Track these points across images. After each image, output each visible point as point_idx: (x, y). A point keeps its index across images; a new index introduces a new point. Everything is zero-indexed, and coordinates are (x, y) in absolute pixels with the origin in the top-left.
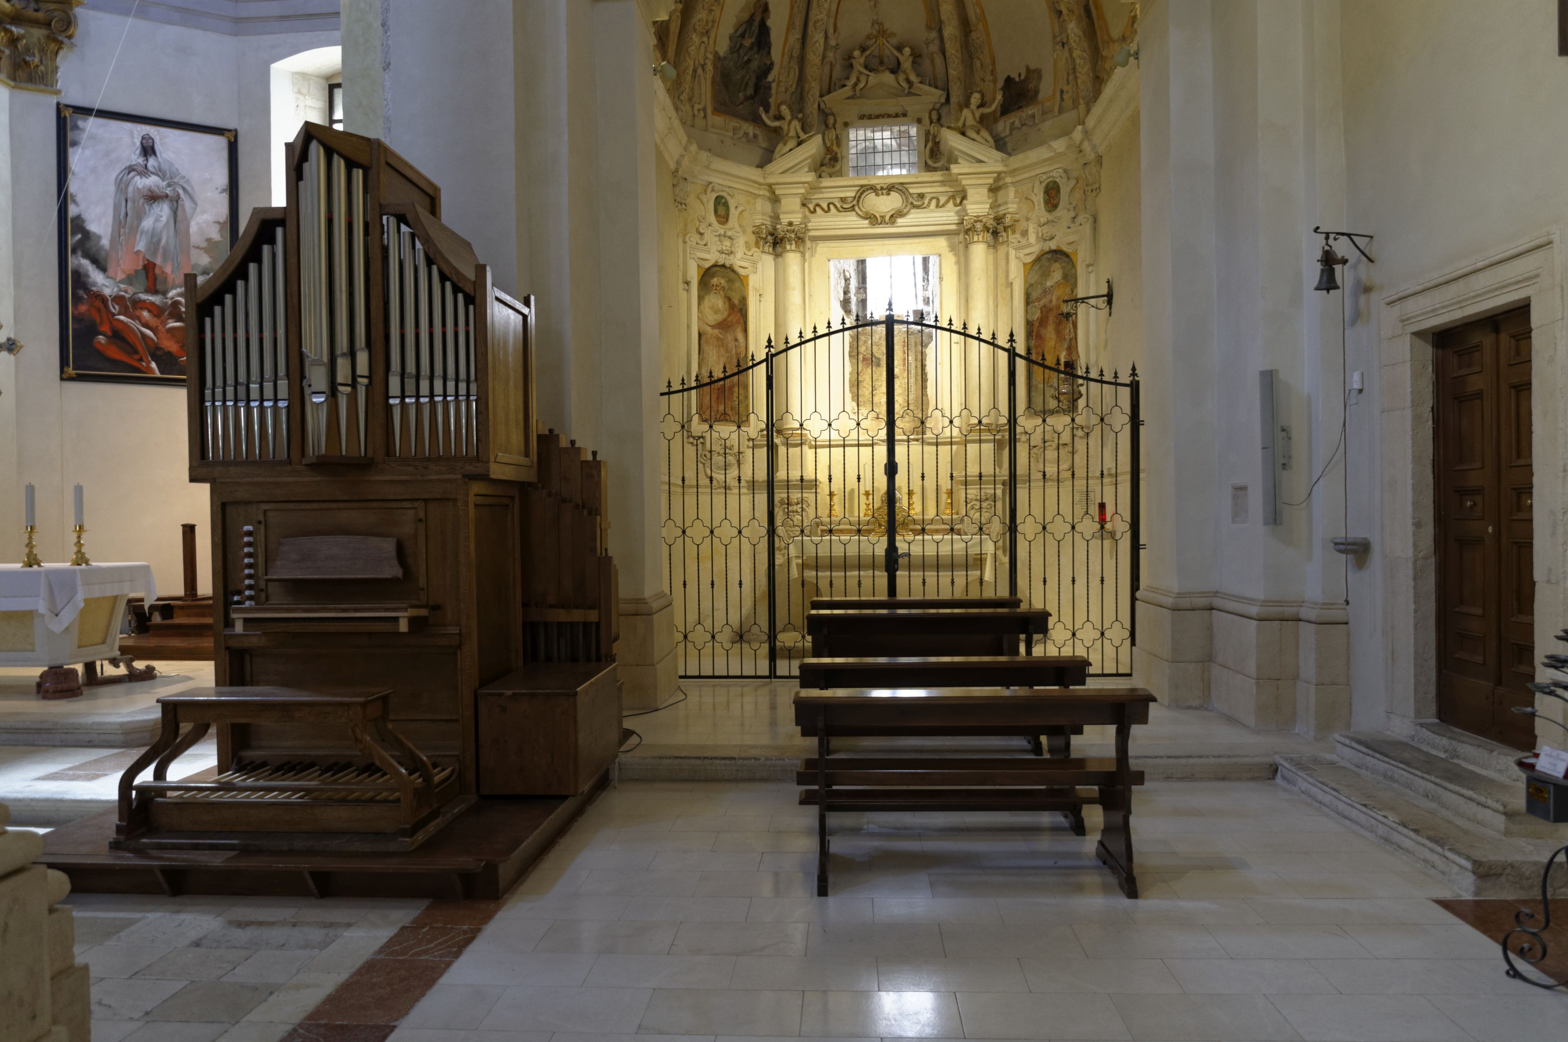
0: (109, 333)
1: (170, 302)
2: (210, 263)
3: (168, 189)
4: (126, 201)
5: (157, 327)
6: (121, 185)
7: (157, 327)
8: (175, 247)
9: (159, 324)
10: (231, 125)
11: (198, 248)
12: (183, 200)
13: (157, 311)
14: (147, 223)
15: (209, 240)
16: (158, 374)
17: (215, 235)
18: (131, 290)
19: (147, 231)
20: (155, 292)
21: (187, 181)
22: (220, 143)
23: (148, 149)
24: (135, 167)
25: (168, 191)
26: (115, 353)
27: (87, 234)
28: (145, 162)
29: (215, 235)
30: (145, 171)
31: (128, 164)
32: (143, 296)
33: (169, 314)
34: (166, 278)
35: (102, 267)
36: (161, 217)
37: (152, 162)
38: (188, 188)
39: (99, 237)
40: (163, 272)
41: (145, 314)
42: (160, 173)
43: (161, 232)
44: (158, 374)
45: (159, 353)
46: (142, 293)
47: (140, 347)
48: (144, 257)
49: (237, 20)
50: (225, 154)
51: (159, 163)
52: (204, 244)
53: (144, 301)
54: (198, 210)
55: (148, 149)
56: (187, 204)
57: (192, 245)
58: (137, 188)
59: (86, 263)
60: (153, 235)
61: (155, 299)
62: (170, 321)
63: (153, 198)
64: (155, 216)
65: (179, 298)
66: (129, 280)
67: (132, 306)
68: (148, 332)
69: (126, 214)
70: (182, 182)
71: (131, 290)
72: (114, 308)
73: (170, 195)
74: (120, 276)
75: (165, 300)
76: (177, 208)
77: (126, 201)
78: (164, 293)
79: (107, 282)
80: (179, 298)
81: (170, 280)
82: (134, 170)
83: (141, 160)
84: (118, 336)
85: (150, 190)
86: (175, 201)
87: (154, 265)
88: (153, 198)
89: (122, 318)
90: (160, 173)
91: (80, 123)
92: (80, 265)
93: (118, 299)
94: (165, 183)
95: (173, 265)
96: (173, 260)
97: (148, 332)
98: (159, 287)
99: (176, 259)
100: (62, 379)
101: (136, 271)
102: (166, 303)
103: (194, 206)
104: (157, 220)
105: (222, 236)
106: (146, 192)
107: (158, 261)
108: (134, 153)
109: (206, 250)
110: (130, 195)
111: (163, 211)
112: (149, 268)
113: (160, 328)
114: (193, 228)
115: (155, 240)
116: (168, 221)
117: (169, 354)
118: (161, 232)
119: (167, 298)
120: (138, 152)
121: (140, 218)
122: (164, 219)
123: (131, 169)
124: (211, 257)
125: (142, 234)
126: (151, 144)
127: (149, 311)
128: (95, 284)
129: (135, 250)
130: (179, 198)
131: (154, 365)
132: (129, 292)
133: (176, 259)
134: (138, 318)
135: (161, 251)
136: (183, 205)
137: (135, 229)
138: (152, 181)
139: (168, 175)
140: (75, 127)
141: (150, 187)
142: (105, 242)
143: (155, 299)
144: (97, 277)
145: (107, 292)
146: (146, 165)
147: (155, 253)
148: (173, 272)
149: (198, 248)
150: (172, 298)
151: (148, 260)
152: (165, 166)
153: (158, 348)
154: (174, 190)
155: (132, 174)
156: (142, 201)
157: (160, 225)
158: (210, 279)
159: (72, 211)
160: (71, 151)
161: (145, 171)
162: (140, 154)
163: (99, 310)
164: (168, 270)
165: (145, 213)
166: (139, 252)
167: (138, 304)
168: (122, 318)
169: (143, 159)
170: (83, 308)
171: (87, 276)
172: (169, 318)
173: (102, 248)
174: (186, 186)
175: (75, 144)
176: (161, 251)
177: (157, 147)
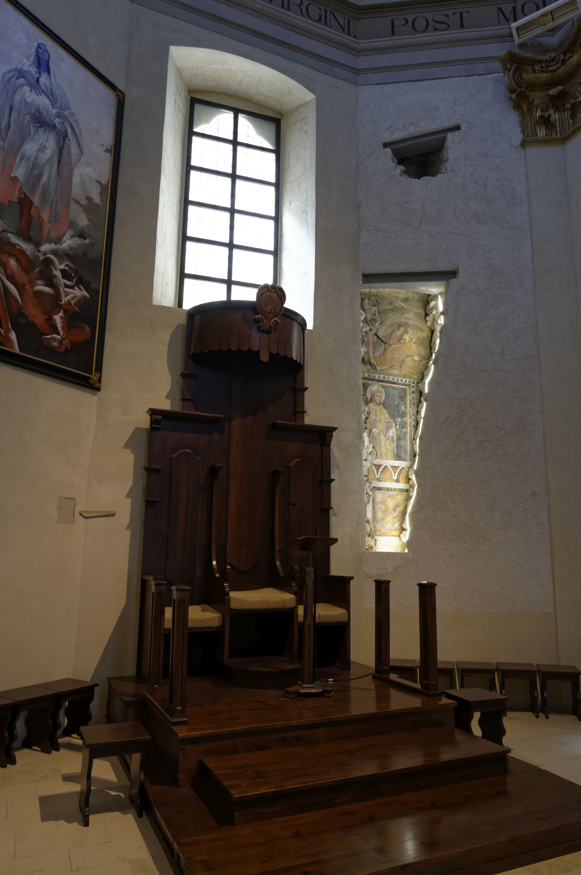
1: (42, 258)
2: (88, 226)
3: (57, 119)
4: (11, 109)
5: (24, 285)
7: (24, 285)
8: (56, 191)
9: (26, 282)
12: (70, 141)
16: (16, 350)
19: (28, 158)
20: (28, 239)
21: (77, 121)
24: (26, 74)
28: (38, 76)
30: (36, 85)
32: (14, 239)
33: (40, 272)
34: (41, 225)
36: (46, 148)
38: (76, 129)
40: (39, 216)
41: (13, 262)
43: (43, 166)
44: (16, 350)
45: (21, 321)
46: (12, 233)
48: (21, 188)
50: (113, 111)
51: (51, 84)
53: (14, 245)
54: (83, 159)
57: (72, 197)
58: (26, 101)
60: (34, 166)
61: (28, 248)
62: (39, 282)
64: (39, 143)
65: (52, 257)
68: (12, 288)
69: (9, 126)
70: (71, 119)
73: (58, 127)
75: (37, 253)
76: (63, 146)
77: (11, 109)
78: (38, 244)
80: (52, 257)
82: (24, 77)
83: (33, 70)
85: (38, 110)
87: (32, 203)
94: (55, 111)
95: (51, 211)
96: (51, 206)
97: (12, 288)
99: (54, 207)
102: (38, 257)
103: (80, 153)
107: (36, 200)
108: (27, 58)
110: (16, 104)
113: (27, 287)
115: (36, 172)
116: (52, 157)
117: (33, 324)
118: (43, 166)
119: (39, 251)
120: (32, 58)
122: (48, 152)
124: (89, 220)
125: (23, 157)
126: (46, 58)
127: (18, 261)
129: (12, 175)
131: (13, 336)
133: (54, 207)
135: (40, 189)
136: (69, 146)
139: (59, 104)
141: (39, 107)
143: (28, 248)
146: (38, 79)
147: (34, 188)
148: (50, 221)
149: (78, 202)
150: (45, 254)
151: (25, 194)
153: (21, 314)
154: (63, 123)
155: (22, 81)
156: (28, 118)
162: (33, 63)
164: (45, 216)
165: (30, 136)
166: (15, 179)
169: (36, 70)
172: (38, 279)
174: (74, 125)
176: (40, 189)
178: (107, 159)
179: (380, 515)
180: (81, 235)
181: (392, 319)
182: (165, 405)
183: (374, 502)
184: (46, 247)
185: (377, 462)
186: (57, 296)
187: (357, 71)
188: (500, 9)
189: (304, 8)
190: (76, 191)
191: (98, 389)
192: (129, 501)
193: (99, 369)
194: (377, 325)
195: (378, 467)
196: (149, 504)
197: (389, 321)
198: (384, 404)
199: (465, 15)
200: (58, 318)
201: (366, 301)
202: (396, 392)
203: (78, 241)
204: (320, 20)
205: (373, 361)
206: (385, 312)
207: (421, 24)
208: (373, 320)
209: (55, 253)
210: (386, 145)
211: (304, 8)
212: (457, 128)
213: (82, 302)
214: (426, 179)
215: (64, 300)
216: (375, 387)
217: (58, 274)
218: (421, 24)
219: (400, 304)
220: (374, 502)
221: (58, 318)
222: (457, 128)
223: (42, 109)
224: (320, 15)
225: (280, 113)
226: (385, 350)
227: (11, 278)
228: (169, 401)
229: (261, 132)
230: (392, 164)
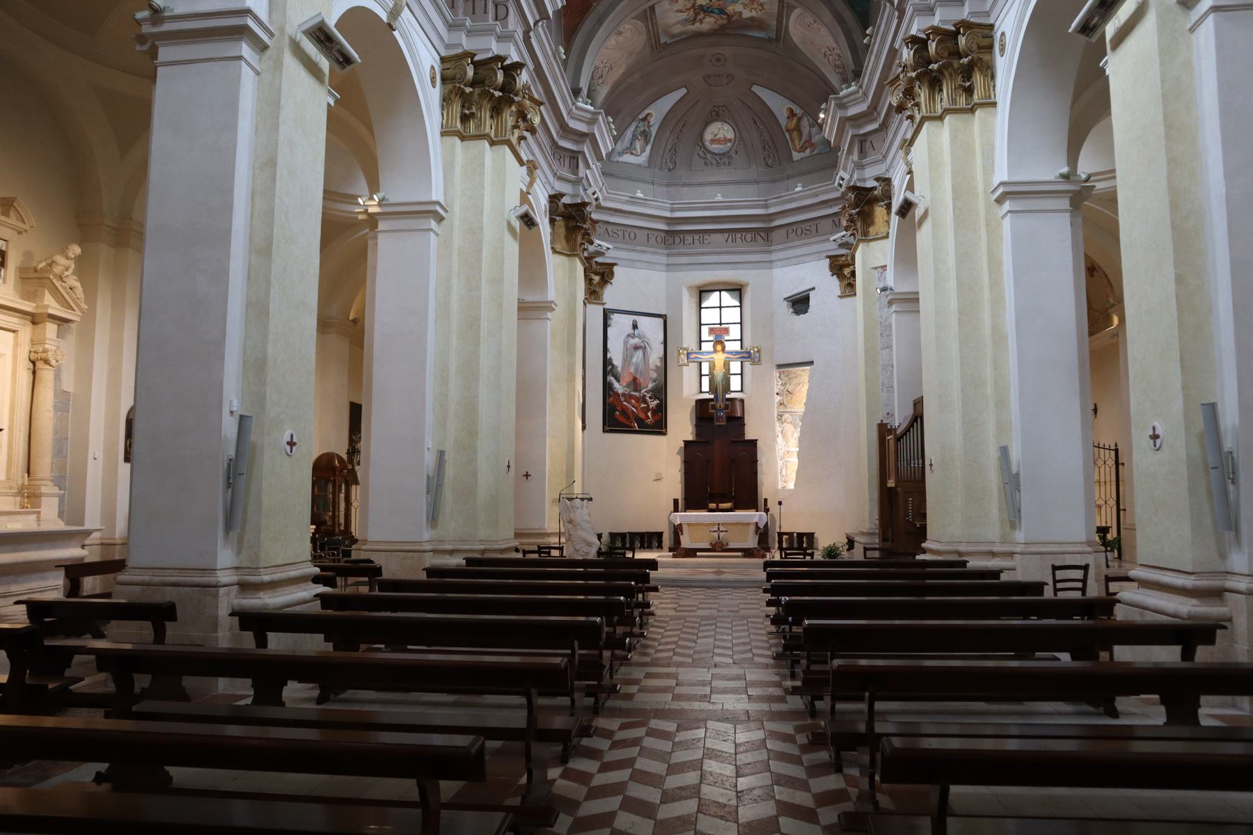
0: (620, 410)
6: (626, 343)
10: (663, 313)
11: (652, 370)
13: (637, 399)
14: (634, 360)
15: (656, 366)
16: (637, 429)
17: (659, 365)
18: (628, 390)
22: (661, 321)
23: (635, 327)
25: (642, 344)
26: (622, 420)
27: (613, 365)
29: (659, 365)
31: (627, 333)
32: (633, 393)
35: (618, 381)
37: (636, 331)
39: (617, 367)
41: (633, 401)
42: (639, 337)
44: (637, 429)
47: (631, 415)
49: (667, 265)
50: (662, 326)
52: (654, 368)
55: (635, 327)
56: (648, 349)
59: (612, 378)
60: (636, 365)
61: (636, 394)
63: (636, 348)
66: (628, 386)
67: (628, 397)
70: (647, 340)
71: (628, 390)
72: (622, 399)
74: (625, 384)
78: (640, 391)
79: (620, 387)
81: (642, 385)
83: (632, 331)
84: (624, 411)
86: (644, 348)
88: (636, 348)
89: (625, 403)
90: (639, 337)
91: (612, 316)
92: (610, 380)
93: (624, 395)
98: (638, 388)
100: (604, 432)
101: (630, 382)
104: (638, 358)
105: (661, 364)
106: (634, 345)
107: (638, 377)
109: (655, 371)
111: (640, 353)
112: (635, 379)
114: (651, 361)
117: (642, 419)
121: (632, 357)
122: (640, 357)
123: (629, 336)
127: (635, 400)
128: (615, 388)
130: (645, 347)
131: (636, 424)
132: (627, 391)
134: (630, 403)
137: (630, 363)
138: (636, 341)
140: (610, 318)
142: (619, 369)
143: (636, 394)
144: (616, 385)
145: (620, 391)
147: (637, 374)
152: (641, 334)
157: (639, 360)
158: (656, 385)
159: (609, 355)
160: (608, 328)
161: (633, 336)
163: (617, 400)
164: (641, 381)
167: (631, 397)
168: (625, 403)
170: (611, 399)
171: (613, 384)
173: (618, 372)
175: (609, 326)
177: (638, 325)
178: (662, 346)
179: (789, 473)
180: (655, 381)
181: (795, 381)
182: (690, 438)
183: (786, 467)
184: (642, 392)
185: (788, 450)
186: (648, 406)
187: (771, 262)
188: (833, 221)
189: (743, 238)
190: (652, 366)
191: (666, 434)
192: (680, 473)
193: (666, 427)
194: (788, 385)
195: (788, 452)
196: (685, 473)
197: (793, 383)
198: (791, 423)
199: (818, 225)
200: (649, 414)
201: (782, 375)
202: (797, 417)
203: (653, 384)
204: (752, 241)
205: (785, 403)
206: (792, 378)
207: (799, 232)
208: (786, 384)
209: (646, 392)
210: (785, 299)
211: (743, 238)
212: (814, 289)
213: (658, 405)
214: (801, 315)
215: (651, 407)
216: (786, 416)
217: (648, 399)
218: (799, 232)
219: (800, 372)
220: (786, 467)
221: (649, 414)
222: (814, 289)
223: (637, 344)
224: (752, 238)
225: (742, 285)
226: (792, 397)
227: (633, 406)
228: (691, 436)
229: (732, 297)
230: (787, 310)
